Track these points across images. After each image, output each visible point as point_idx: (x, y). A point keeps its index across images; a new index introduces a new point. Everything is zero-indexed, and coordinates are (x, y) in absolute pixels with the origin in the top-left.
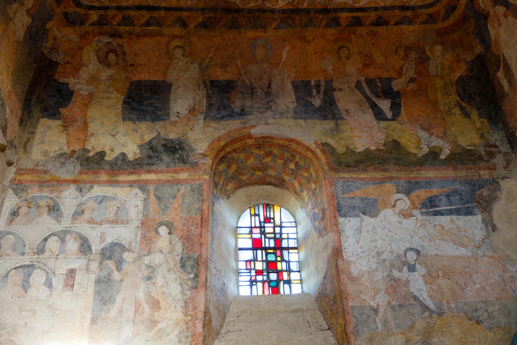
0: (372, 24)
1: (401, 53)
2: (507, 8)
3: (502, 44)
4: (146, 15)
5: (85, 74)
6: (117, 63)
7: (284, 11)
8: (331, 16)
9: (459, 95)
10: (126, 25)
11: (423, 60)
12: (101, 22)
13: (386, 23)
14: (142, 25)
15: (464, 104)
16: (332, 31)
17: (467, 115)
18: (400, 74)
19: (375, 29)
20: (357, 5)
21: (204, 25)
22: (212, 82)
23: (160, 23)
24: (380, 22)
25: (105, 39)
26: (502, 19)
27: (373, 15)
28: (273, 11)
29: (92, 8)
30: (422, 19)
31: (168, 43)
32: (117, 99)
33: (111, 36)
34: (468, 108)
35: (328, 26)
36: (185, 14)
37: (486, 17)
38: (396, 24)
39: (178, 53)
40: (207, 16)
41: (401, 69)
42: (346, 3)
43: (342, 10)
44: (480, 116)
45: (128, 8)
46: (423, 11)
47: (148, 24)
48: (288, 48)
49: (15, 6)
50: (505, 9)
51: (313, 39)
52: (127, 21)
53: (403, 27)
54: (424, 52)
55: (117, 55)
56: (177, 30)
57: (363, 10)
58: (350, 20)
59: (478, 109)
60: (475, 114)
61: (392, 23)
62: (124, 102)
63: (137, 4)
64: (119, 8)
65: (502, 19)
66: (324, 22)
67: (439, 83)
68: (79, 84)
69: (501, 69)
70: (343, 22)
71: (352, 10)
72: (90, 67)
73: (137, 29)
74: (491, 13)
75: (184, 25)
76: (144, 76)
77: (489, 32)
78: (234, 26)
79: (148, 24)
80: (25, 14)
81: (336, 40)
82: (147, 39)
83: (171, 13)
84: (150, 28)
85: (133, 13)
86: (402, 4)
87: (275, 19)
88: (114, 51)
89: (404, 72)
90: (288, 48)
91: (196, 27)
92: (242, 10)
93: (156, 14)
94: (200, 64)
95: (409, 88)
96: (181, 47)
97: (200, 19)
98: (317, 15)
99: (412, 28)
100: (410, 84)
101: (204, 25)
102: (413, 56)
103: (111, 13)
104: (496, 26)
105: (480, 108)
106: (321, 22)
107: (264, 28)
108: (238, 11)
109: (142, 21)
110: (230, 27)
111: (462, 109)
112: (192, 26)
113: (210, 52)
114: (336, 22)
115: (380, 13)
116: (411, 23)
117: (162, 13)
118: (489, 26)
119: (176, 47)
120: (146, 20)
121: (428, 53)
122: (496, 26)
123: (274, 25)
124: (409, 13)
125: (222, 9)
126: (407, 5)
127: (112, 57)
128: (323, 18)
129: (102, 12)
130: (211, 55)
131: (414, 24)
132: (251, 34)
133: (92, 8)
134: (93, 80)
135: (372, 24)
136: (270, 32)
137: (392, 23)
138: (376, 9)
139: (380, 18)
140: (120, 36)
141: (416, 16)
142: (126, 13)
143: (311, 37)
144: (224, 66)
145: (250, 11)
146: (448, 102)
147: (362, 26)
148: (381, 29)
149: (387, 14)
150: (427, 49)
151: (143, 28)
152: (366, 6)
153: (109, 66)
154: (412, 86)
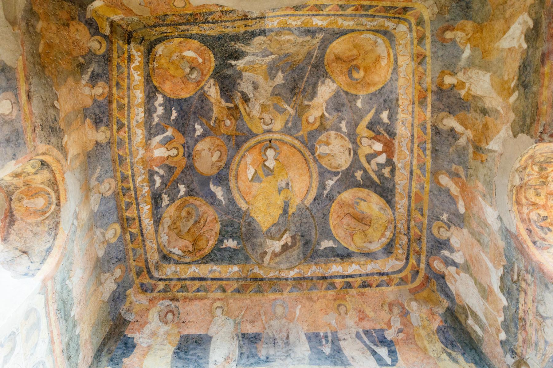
0: (360, 287)
1: (386, 308)
2: (457, 267)
3: (463, 296)
4: (197, 284)
5: (147, 330)
6: (173, 321)
7: (295, 279)
8: (329, 281)
9: (442, 342)
10: (183, 292)
11: (405, 314)
12: (165, 291)
13: (370, 286)
14: (194, 291)
15: (449, 351)
16: (331, 293)
17: (455, 361)
18: (390, 327)
19: (363, 290)
20: (346, 273)
21: (238, 291)
22: (243, 334)
23: (206, 290)
24: (365, 285)
25: (167, 302)
26: (456, 276)
27: (359, 280)
28: (286, 279)
29: (160, 280)
30: (395, 282)
31: (212, 304)
32: (169, 349)
33: (171, 300)
34: (454, 354)
35: (327, 289)
36: (225, 282)
37: (443, 277)
38: (377, 286)
39: (219, 312)
40: (240, 284)
41: (389, 321)
42: (338, 272)
43: (336, 277)
44: (466, 360)
45: (185, 279)
46: (395, 275)
47: (198, 290)
48: (299, 307)
49: (107, 275)
50: (455, 268)
51: (318, 299)
52: (184, 288)
53: (383, 288)
54: (404, 308)
55: (174, 314)
56: (219, 294)
57: (351, 276)
58: (343, 284)
59: (463, 354)
60: (461, 359)
61: (374, 285)
62: (174, 353)
63: (192, 276)
64: (179, 279)
65: (456, 276)
66: (324, 287)
67: (423, 333)
68: (140, 338)
69: (470, 317)
70: (338, 285)
71: (343, 277)
72: (153, 324)
73: (190, 295)
74: (446, 273)
75: (224, 291)
76: (192, 331)
77: (449, 288)
78: (260, 291)
79: (198, 290)
80: (113, 281)
81: (335, 300)
82: (196, 302)
83: (215, 282)
84: (199, 293)
85: (188, 283)
86: (379, 271)
87: (288, 285)
88: (172, 311)
89: (392, 324)
90: (299, 307)
91: (232, 292)
92: (265, 279)
93: (204, 283)
94: (235, 321)
95: (400, 338)
96: (221, 307)
97: (235, 286)
98: (318, 281)
99: (390, 289)
100: (400, 334)
101: (238, 291)
102: (396, 310)
103: (173, 283)
104: (453, 282)
105: (464, 354)
106: (322, 286)
107: (281, 291)
108: (262, 280)
109: (194, 288)
110: (257, 292)
111: (449, 355)
112: (229, 291)
113: (242, 311)
114: (333, 286)
115: (364, 278)
116: (388, 285)
117: (209, 282)
118: (448, 283)
119: (217, 308)
120: (197, 287)
121: (407, 308)
122: (453, 282)
123: (288, 289)
124: (385, 278)
125: (251, 278)
126: (382, 272)
127: (170, 316)
128: (323, 283)
129: (167, 283)
130: (243, 313)
131: (391, 286)
132: (272, 296)
133: (160, 280)
134: (154, 334)
135: (360, 287)
136: (286, 294)
137: (374, 285)
138: (360, 275)
139: (364, 282)
140: (178, 300)
141: (391, 280)
142: (184, 283)
143: (316, 298)
144: (252, 322)
145: (270, 279)
146: (435, 349)
147: (352, 288)
148: (367, 290)
149: (369, 279)
150: (405, 304)
151: (194, 294)
152: (353, 273)
153: (166, 323)
154: (401, 335)
